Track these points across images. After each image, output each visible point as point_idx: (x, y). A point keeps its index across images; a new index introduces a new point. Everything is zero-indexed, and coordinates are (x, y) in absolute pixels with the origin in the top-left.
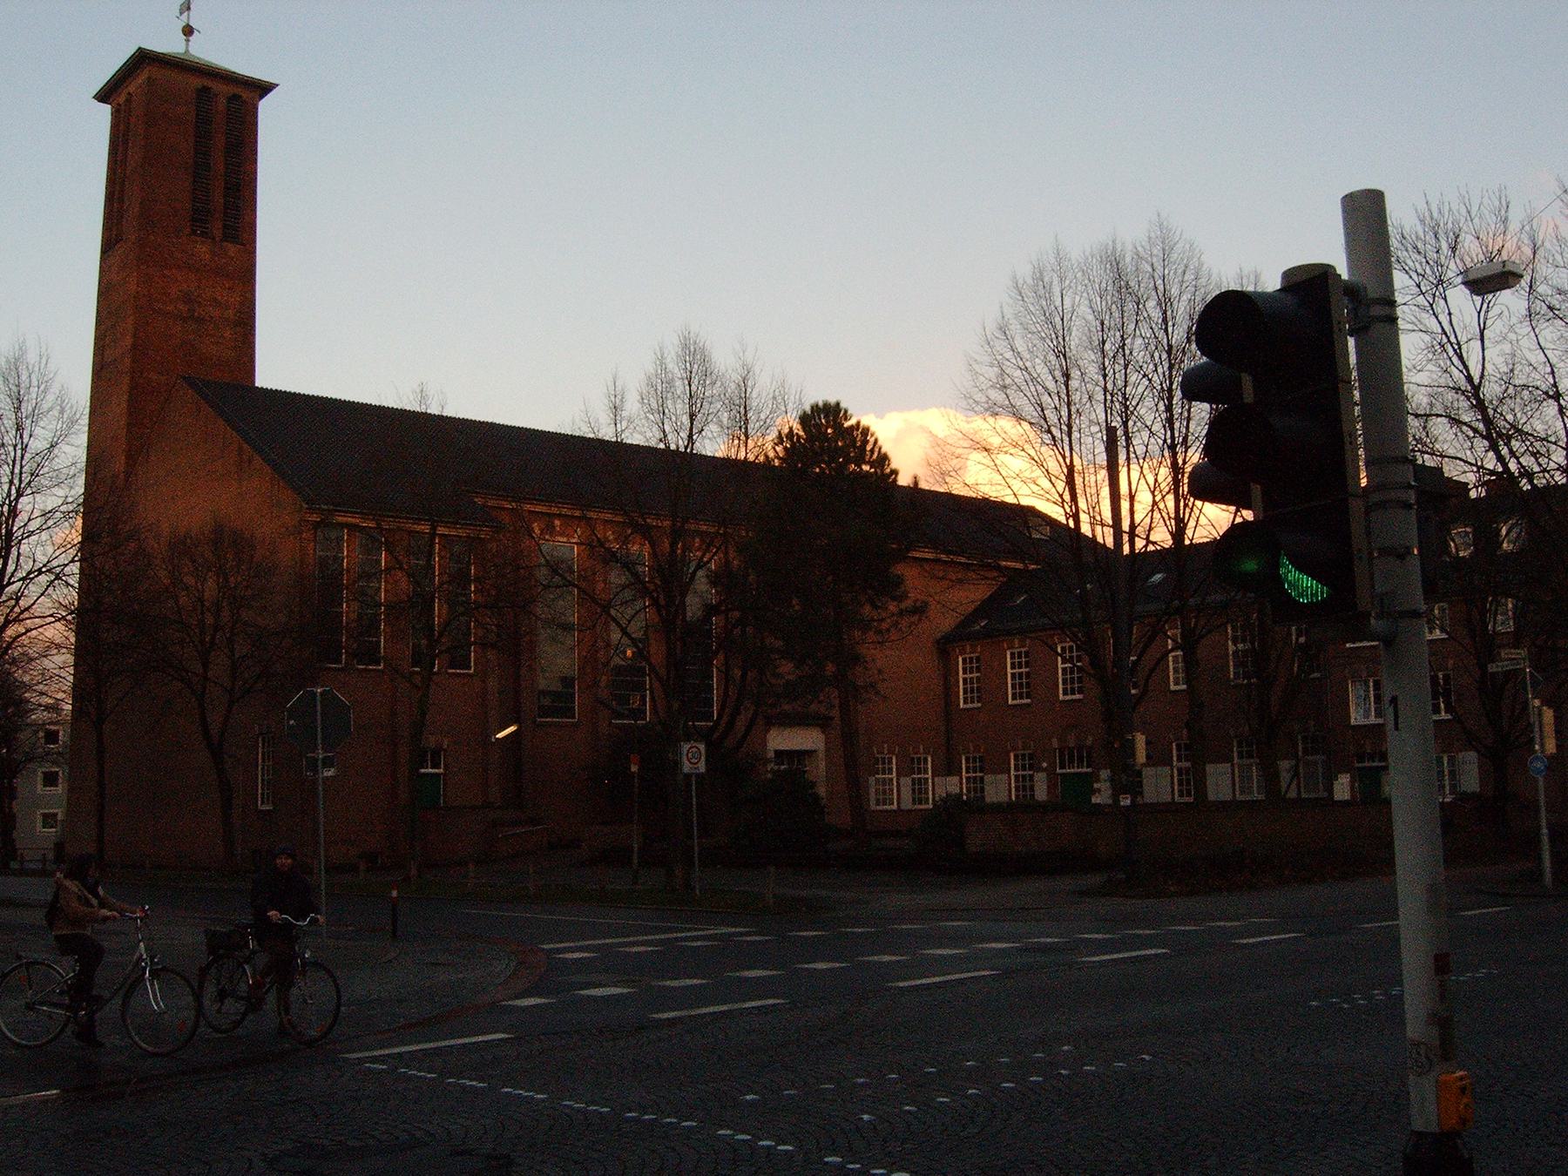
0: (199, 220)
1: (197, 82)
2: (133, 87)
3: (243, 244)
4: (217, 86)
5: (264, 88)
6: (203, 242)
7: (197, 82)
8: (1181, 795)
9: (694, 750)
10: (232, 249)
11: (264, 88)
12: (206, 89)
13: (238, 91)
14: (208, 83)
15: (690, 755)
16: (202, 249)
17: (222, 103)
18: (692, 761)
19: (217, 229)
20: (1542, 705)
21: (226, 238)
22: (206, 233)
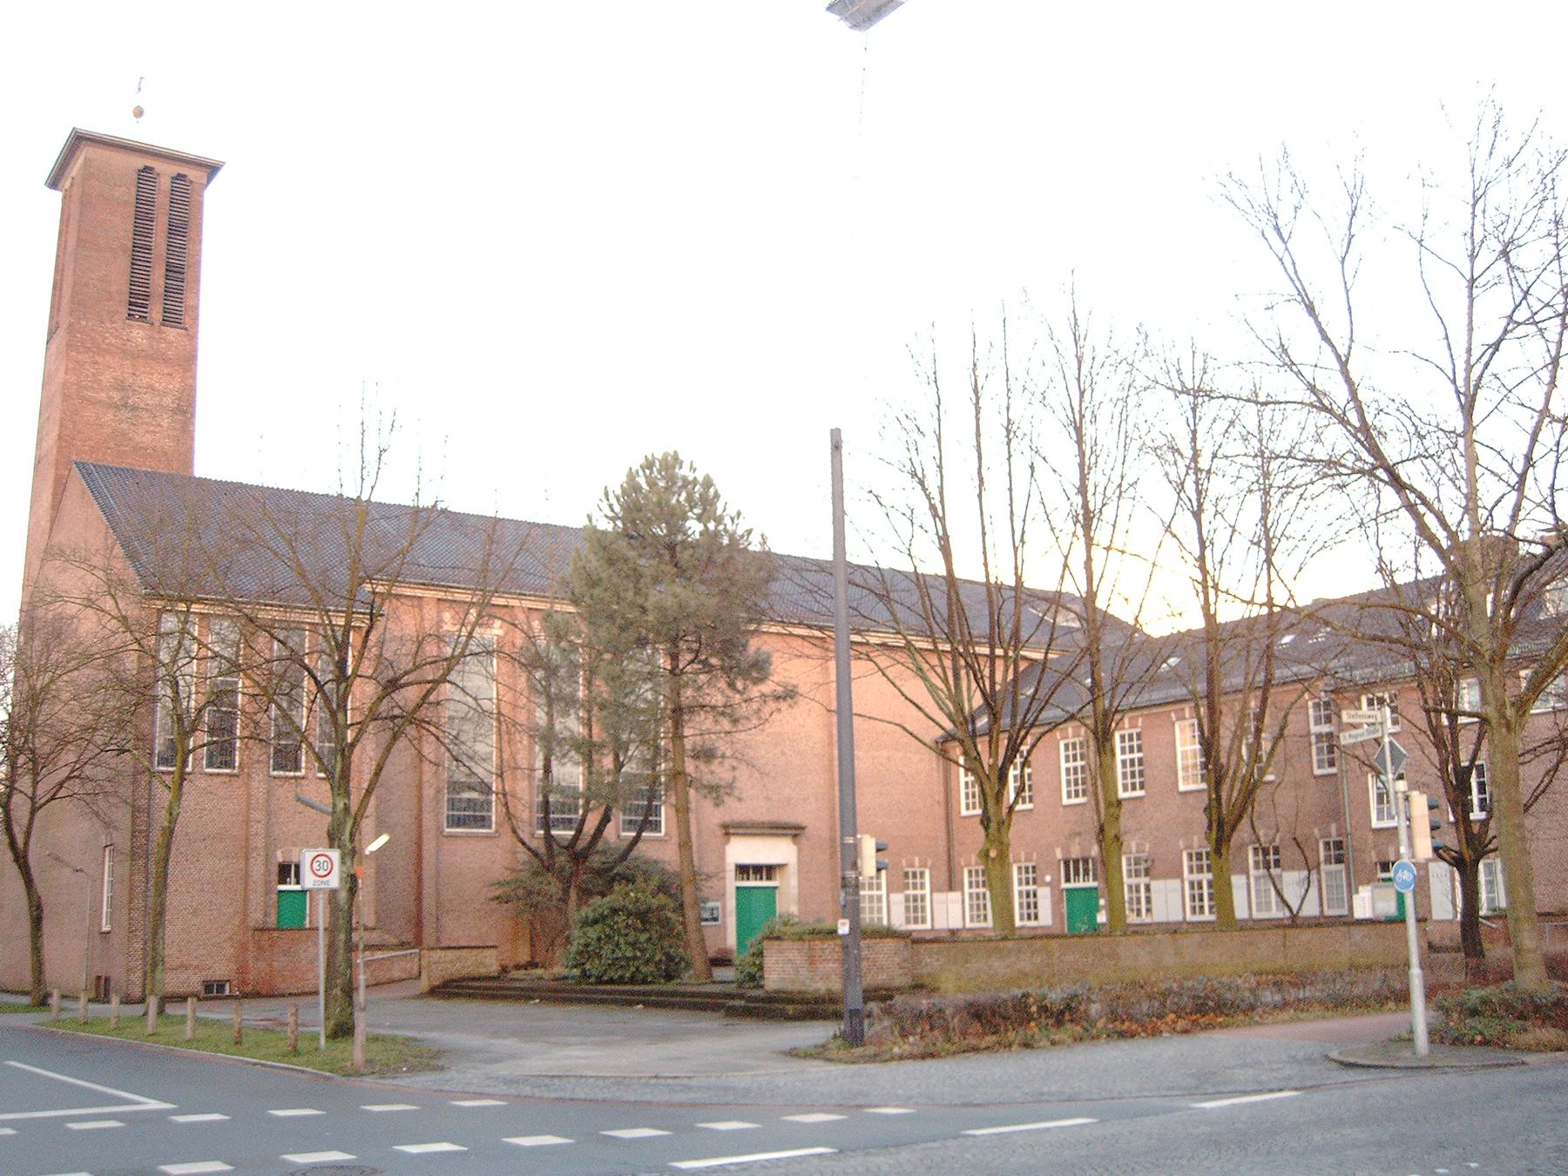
0: (137, 304)
1: (141, 162)
2: (75, 169)
3: (186, 329)
4: (158, 166)
5: (212, 169)
6: (141, 327)
7: (141, 162)
8: (972, 920)
9: (322, 859)
10: (172, 333)
11: (212, 169)
12: (147, 169)
13: (150, 163)
14: (150, 163)
15: (315, 865)
16: (138, 334)
17: (165, 184)
18: (319, 873)
19: (156, 313)
20: (1410, 789)
21: (165, 321)
22: (145, 317)
